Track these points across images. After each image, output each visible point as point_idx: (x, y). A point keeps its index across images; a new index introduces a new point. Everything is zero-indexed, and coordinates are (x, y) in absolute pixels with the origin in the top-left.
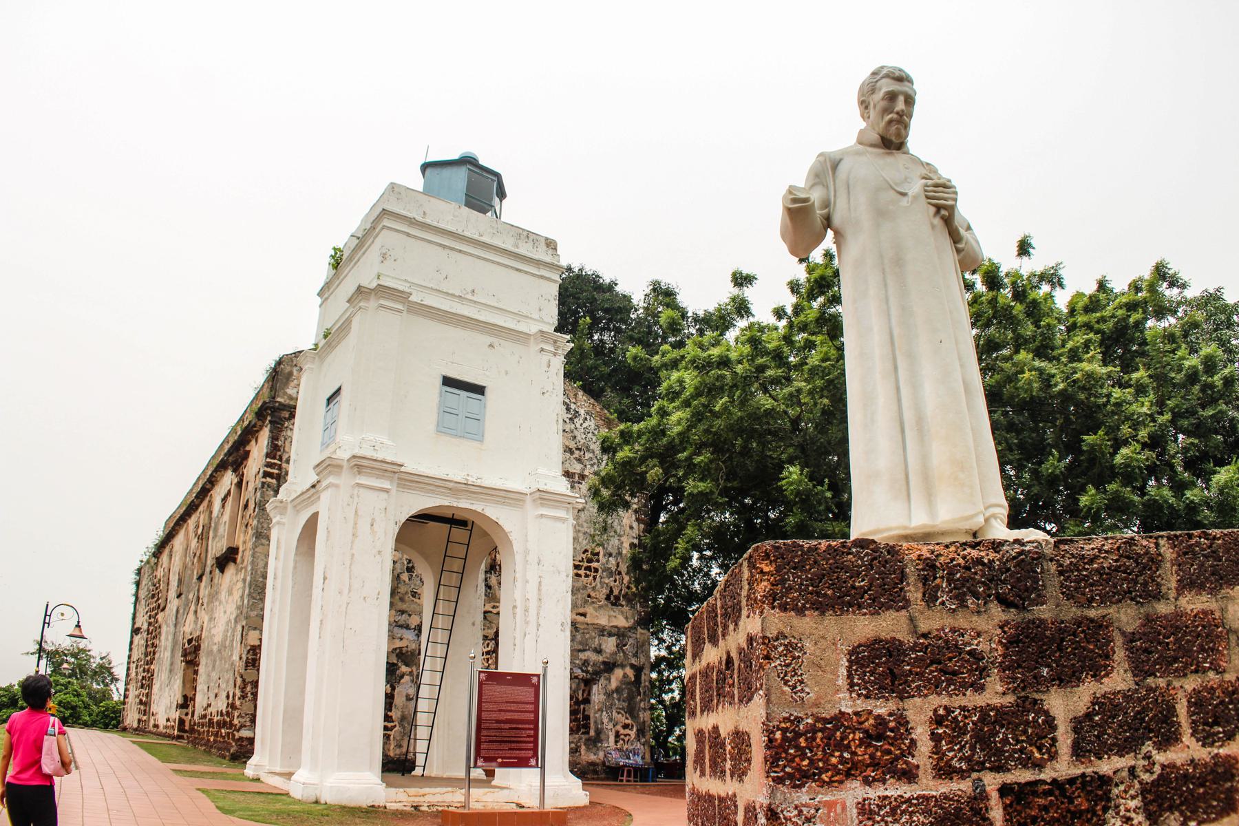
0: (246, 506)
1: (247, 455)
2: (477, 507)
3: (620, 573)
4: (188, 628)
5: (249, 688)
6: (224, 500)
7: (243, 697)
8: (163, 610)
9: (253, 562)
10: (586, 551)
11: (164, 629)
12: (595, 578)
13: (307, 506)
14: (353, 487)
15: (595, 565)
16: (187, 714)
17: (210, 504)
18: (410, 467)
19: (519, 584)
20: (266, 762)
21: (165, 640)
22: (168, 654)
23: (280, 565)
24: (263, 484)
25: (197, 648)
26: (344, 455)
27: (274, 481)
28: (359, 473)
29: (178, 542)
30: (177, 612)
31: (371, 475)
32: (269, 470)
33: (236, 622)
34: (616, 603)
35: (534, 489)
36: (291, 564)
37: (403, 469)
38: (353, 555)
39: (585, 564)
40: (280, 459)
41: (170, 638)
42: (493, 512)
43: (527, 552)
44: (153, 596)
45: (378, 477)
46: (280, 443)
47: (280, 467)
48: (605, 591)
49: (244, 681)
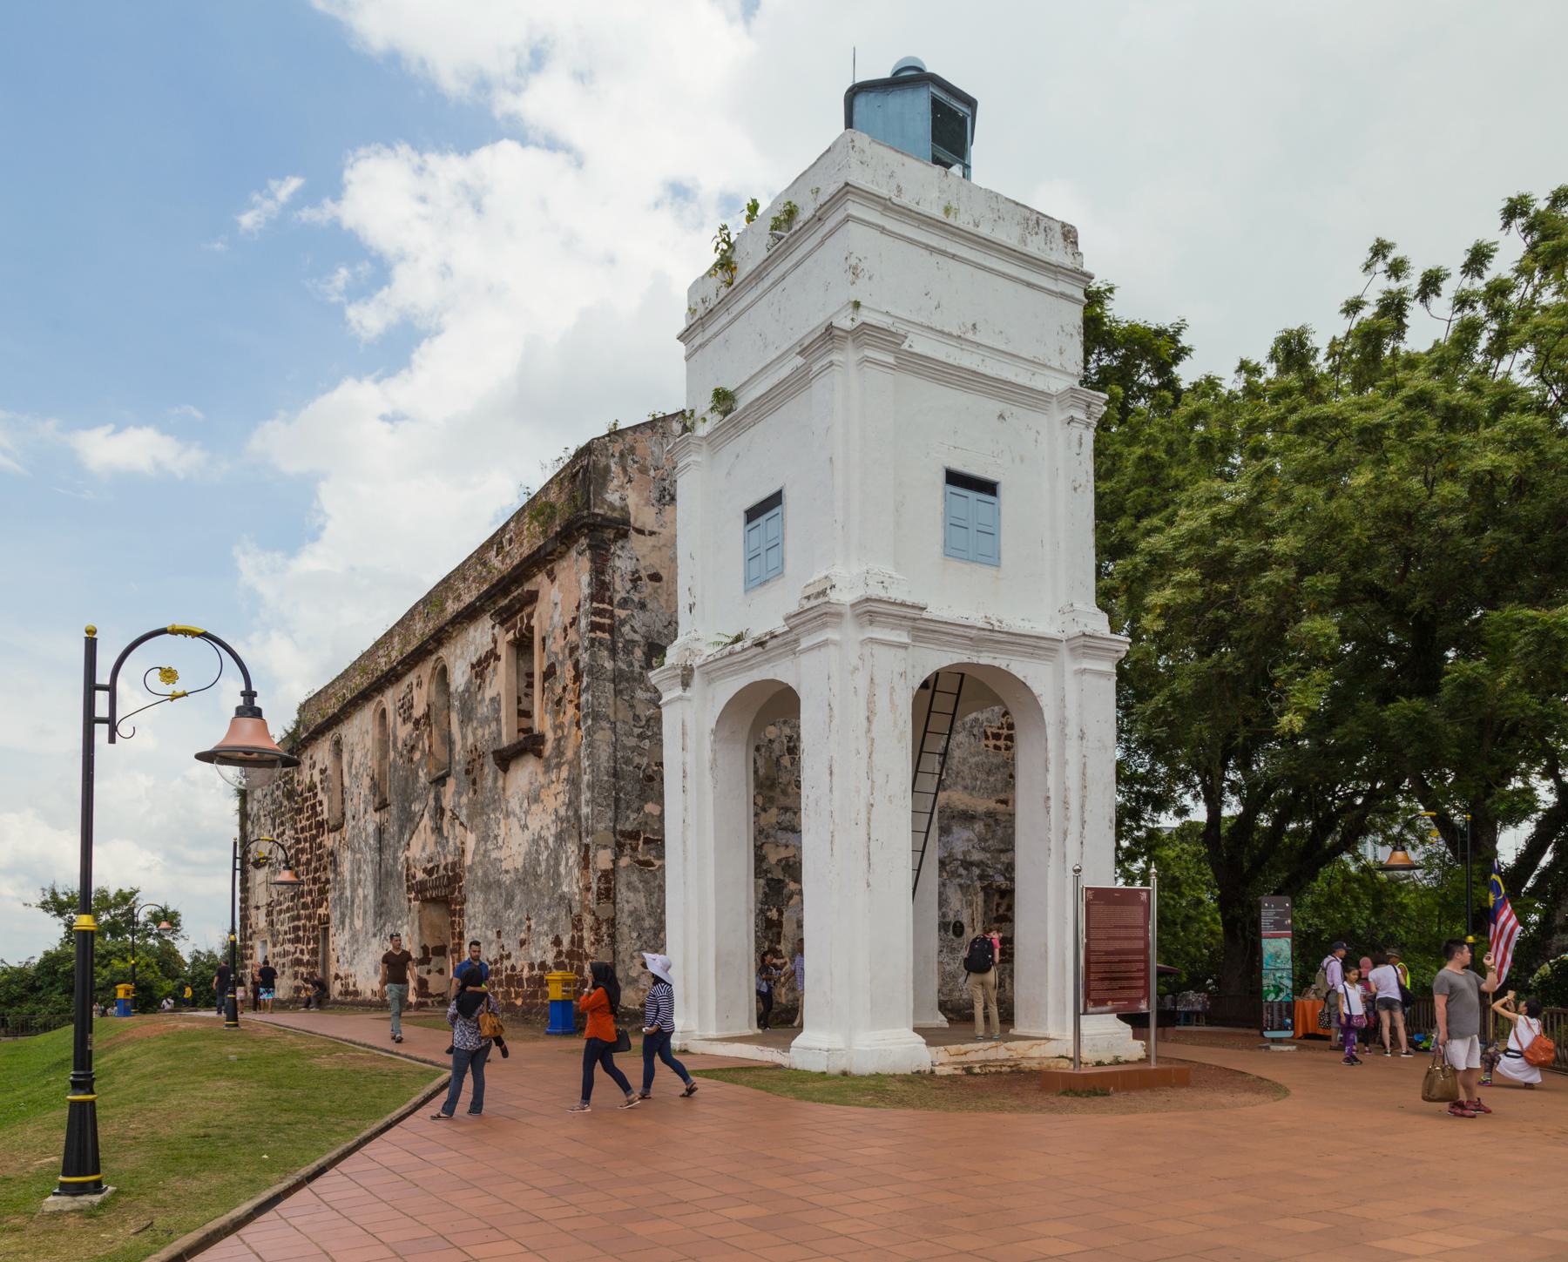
0: (549, 673)
1: (533, 597)
2: (1001, 662)
4: (420, 848)
5: (604, 929)
6: (480, 667)
7: (598, 941)
8: (338, 827)
9: (590, 756)
11: (346, 859)
13: (735, 673)
14: (863, 643)
16: (429, 972)
17: (443, 674)
18: (934, 612)
19: (1052, 767)
20: (694, 1026)
21: (355, 871)
22: (367, 891)
23: (690, 758)
24: (592, 641)
25: (457, 878)
26: (844, 596)
27: (607, 636)
28: (871, 623)
29: (360, 731)
30: (380, 831)
31: (885, 625)
32: (597, 619)
33: (560, 837)
35: (1075, 630)
36: (708, 755)
37: (925, 615)
38: (873, 740)
40: (611, 603)
41: (368, 869)
42: (1019, 667)
43: (1063, 723)
44: (299, 811)
45: (894, 627)
46: (607, 579)
47: (612, 616)
49: (597, 919)
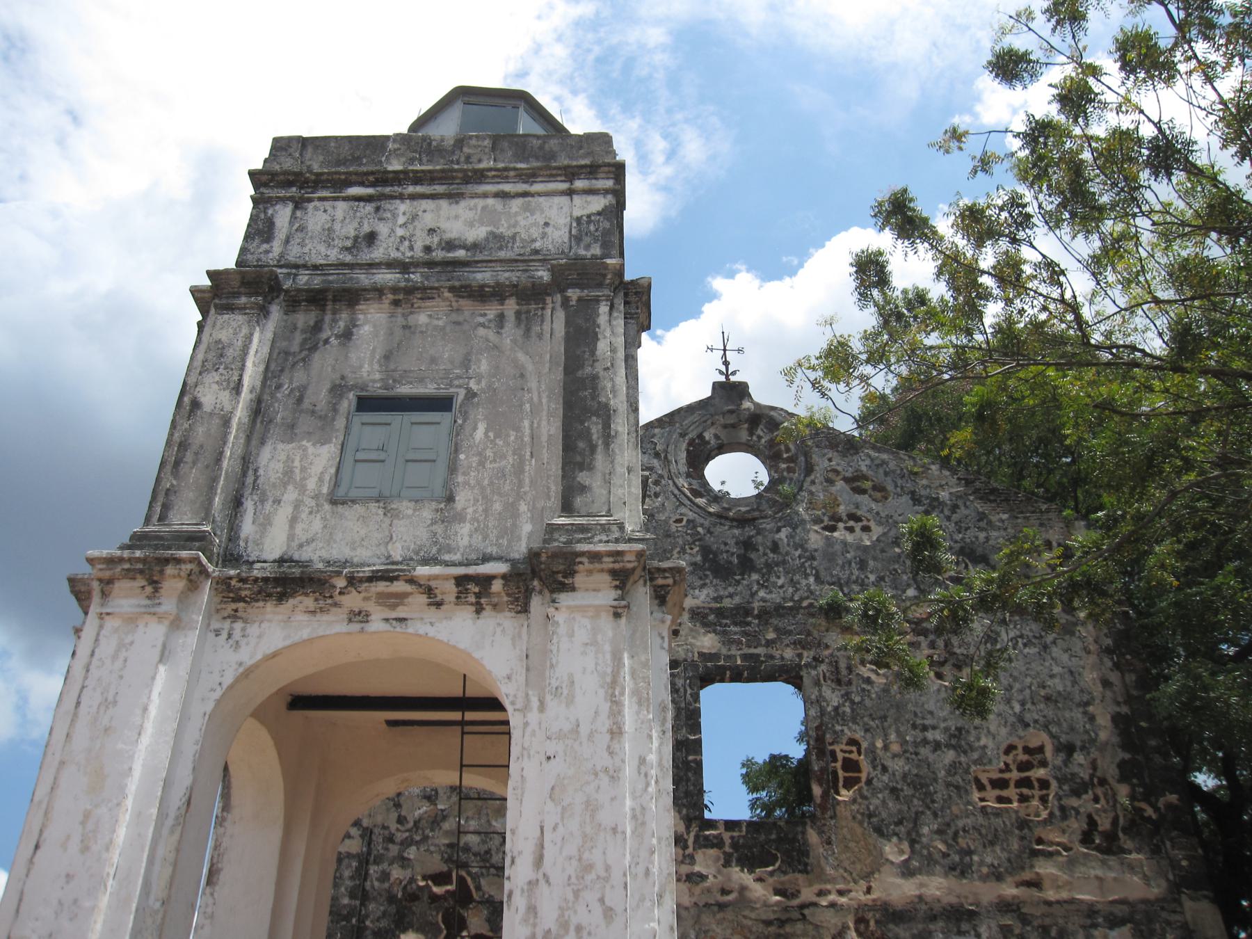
3: (1103, 782)
10: (1010, 749)
12: (1044, 800)
15: (1041, 773)
34: (1110, 847)
39: (1015, 775)
48: (1077, 825)
